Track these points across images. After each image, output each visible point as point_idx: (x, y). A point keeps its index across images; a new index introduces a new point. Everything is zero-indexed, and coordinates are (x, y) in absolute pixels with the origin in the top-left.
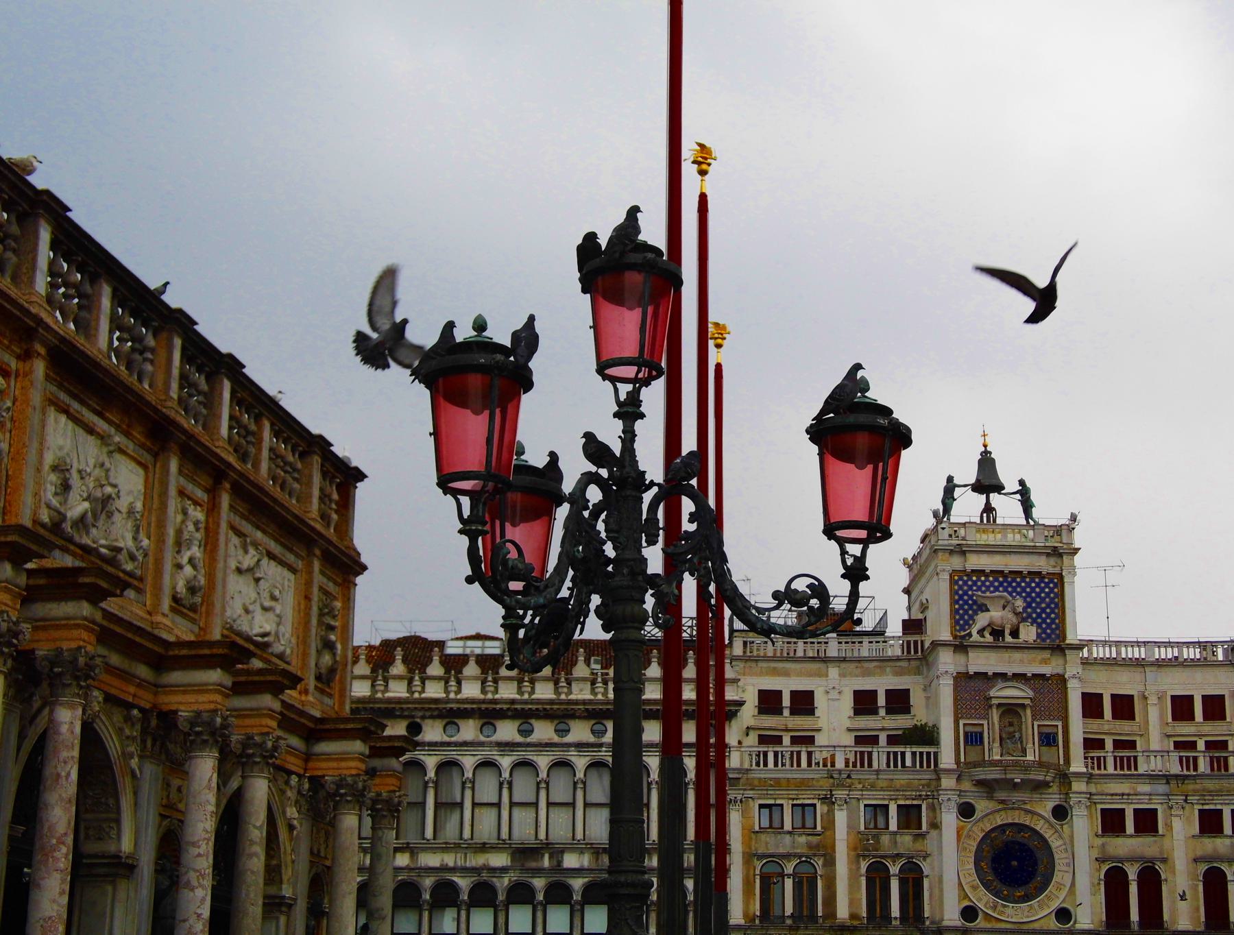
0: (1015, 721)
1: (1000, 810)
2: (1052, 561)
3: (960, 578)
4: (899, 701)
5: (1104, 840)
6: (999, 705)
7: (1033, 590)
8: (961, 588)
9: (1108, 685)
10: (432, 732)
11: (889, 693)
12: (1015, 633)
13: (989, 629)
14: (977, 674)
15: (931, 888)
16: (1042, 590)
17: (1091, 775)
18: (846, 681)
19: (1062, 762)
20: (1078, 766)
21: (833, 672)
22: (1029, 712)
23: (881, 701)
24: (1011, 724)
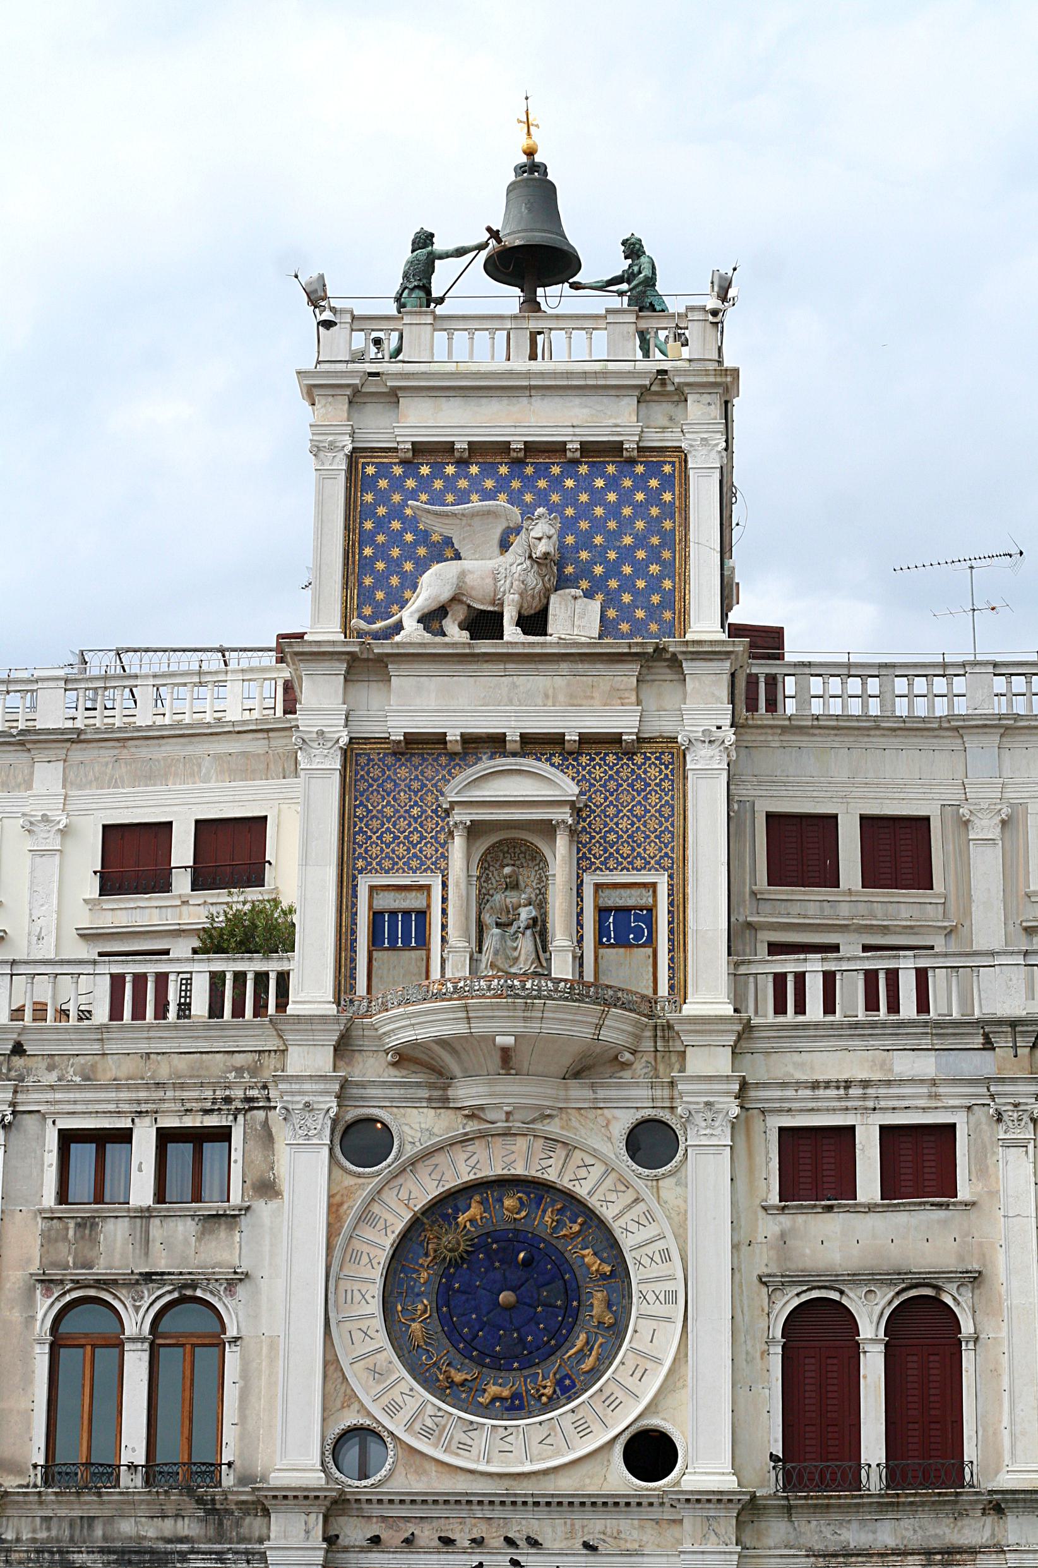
0: (528, 877)
1: (465, 1140)
2: (659, 413)
4: (233, 850)
5: (785, 1220)
6: (474, 830)
9: (849, 791)
11: (202, 826)
12: (534, 622)
14: (413, 741)
15: (245, 1374)
16: (626, 497)
18: (83, 798)
19: (663, 990)
20: (709, 997)
21: (48, 776)
22: (562, 841)
23: (182, 851)
24: (513, 885)
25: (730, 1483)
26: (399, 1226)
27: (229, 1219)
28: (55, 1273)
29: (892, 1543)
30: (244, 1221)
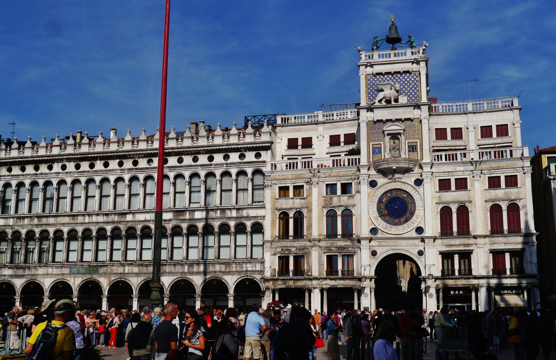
0: (397, 141)
1: (389, 183)
3: (371, 78)
4: (351, 139)
6: (388, 135)
7: (406, 80)
8: (371, 82)
10: (143, 163)
12: (396, 100)
13: (384, 100)
15: (356, 220)
16: (411, 79)
17: (433, 164)
19: (419, 158)
21: (321, 127)
22: (402, 135)
25: (432, 235)
26: (379, 197)
27: (353, 197)
28: (326, 206)
29: (458, 243)
30: (355, 197)
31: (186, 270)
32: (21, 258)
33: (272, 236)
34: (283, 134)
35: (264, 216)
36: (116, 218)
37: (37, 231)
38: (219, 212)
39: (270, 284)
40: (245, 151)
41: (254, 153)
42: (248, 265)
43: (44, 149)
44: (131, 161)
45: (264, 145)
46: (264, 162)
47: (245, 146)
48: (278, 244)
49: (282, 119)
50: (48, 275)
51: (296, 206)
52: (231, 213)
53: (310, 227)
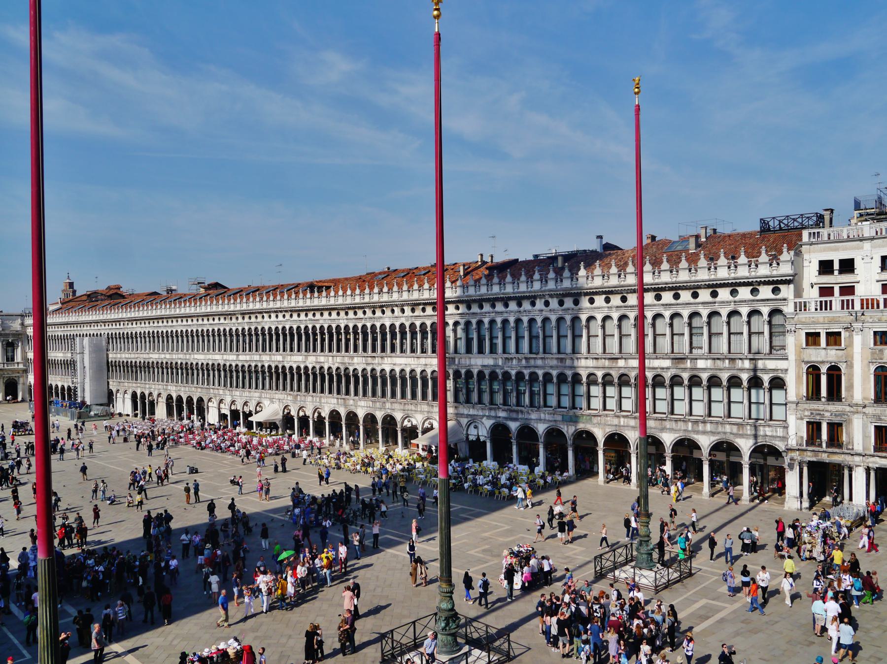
21: (867, 245)
31: (690, 428)
32: (513, 400)
33: (797, 395)
34: (813, 255)
35: (787, 370)
36: (607, 363)
37: (526, 372)
38: (727, 361)
39: (796, 455)
40: (759, 285)
41: (771, 287)
42: (767, 429)
43: (525, 284)
44: (619, 296)
45: (784, 278)
46: (785, 300)
47: (758, 280)
48: (806, 406)
49: (810, 234)
50: (540, 420)
51: (830, 359)
52: (743, 363)
53: (850, 387)
